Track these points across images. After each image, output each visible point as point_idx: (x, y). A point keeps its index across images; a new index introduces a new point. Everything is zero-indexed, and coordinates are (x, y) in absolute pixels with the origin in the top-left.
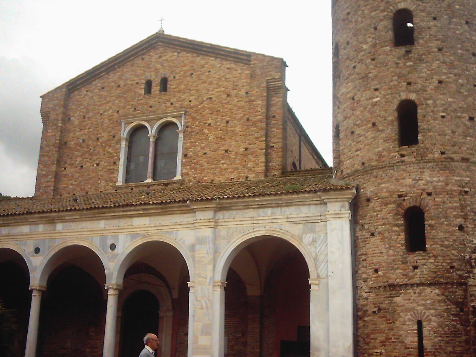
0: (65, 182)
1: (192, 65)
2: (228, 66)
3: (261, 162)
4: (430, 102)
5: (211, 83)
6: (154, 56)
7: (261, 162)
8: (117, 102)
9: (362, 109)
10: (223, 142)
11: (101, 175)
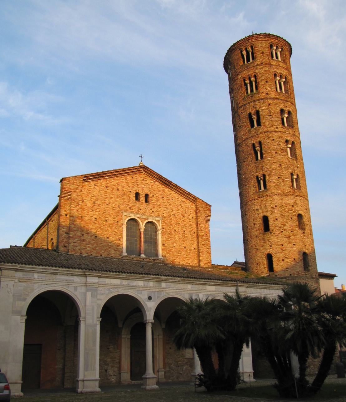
2: (182, 200)
4: (311, 255)
5: (174, 206)
6: (140, 177)
7: (206, 258)
8: (118, 199)
9: (288, 251)
10: (183, 242)
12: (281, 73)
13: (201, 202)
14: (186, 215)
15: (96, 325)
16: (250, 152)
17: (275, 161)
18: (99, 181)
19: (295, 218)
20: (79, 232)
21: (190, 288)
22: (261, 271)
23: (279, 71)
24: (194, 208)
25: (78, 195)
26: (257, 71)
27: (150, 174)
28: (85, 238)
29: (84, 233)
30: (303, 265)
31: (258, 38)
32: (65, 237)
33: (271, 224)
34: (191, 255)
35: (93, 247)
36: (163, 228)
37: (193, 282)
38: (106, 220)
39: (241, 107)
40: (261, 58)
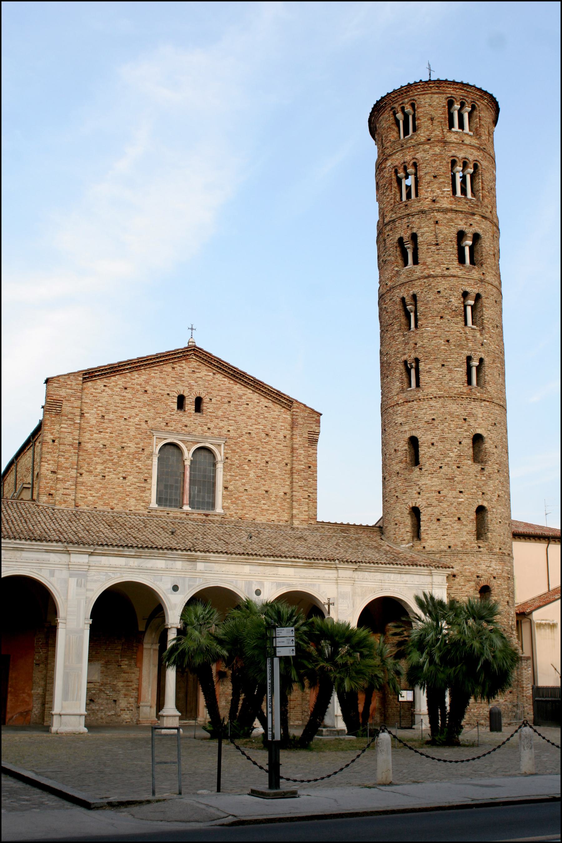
0: (82, 492)
1: (230, 392)
3: (305, 511)
4: (494, 510)
5: (249, 417)
6: (186, 368)
7: (305, 511)
9: (449, 503)
10: (264, 482)
11: (129, 491)
12: (465, 158)
13: (303, 407)
14: (272, 434)
15: (83, 630)
16: (396, 313)
17: (439, 333)
18: (112, 378)
19: (468, 442)
20: (73, 470)
21: (249, 572)
22: (401, 538)
23: (461, 155)
24: (290, 419)
25: (73, 407)
26: (418, 156)
27: (206, 360)
28: (84, 481)
29: (83, 471)
30: (474, 529)
31: (426, 89)
32: (51, 479)
33: (423, 452)
34: (278, 505)
35: (98, 495)
36: (227, 458)
37: (254, 561)
38: (123, 447)
39: (387, 224)
40: (428, 130)
